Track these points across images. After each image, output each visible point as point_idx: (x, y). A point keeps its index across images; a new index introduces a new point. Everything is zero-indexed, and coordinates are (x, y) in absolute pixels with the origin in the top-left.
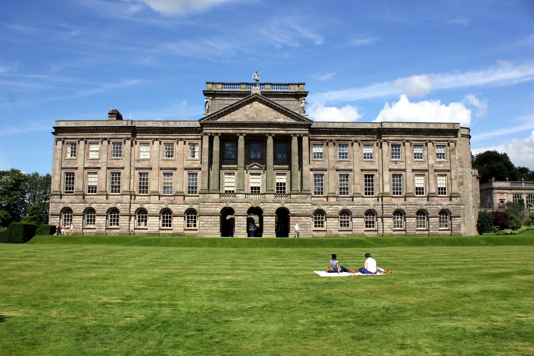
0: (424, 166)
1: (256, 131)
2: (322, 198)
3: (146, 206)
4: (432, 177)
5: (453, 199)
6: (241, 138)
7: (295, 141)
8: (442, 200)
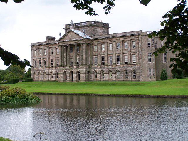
0: (127, 52)
1: (72, 43)
2: (96, 66)
3: (52, 71)
4: (129, 56)
5: (136, 65)
7: (82, 45)
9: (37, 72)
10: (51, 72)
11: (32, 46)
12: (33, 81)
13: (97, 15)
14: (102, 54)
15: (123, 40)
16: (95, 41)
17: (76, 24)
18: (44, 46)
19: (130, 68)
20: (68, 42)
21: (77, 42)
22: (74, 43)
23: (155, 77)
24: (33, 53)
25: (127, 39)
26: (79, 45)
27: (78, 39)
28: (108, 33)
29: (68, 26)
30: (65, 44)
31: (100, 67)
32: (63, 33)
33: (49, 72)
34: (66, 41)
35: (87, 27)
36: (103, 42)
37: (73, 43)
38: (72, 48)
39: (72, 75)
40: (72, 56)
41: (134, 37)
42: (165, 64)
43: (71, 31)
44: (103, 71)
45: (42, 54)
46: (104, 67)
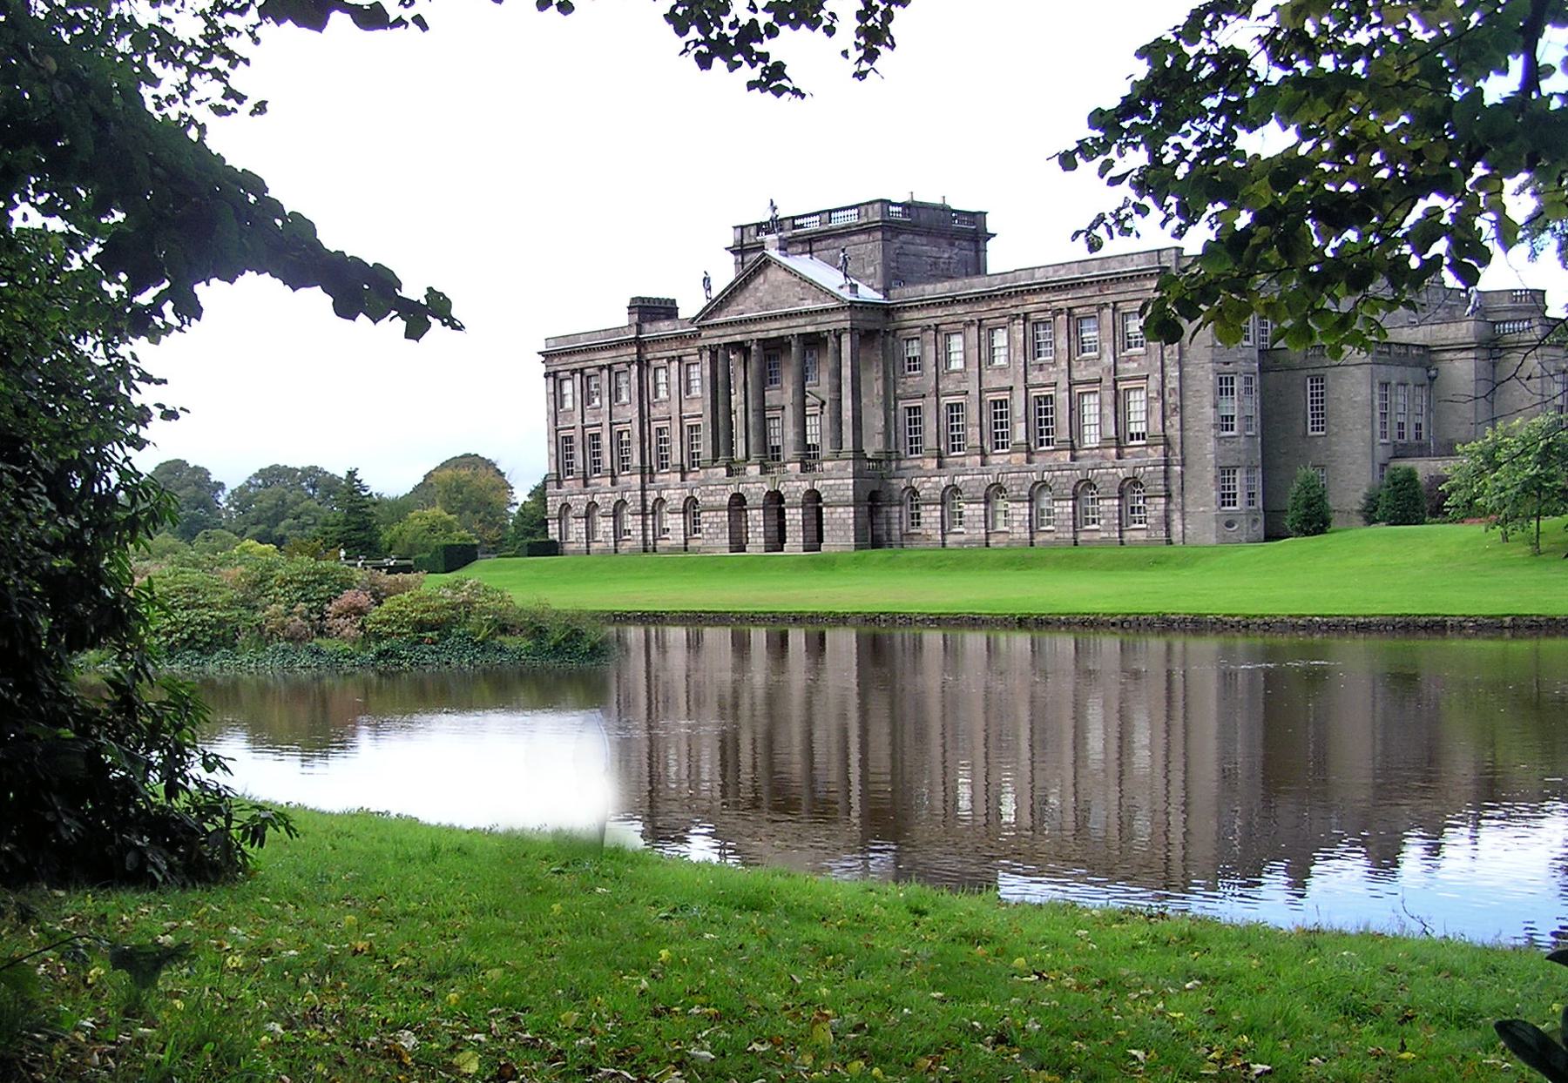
1: (774, 330)
3: (665, 494)
4: (1109, 396)
6: (754, 347)
8: (1134, 456)
9: (579, 504)
10: (660, 501)
11: (547, 356)
12: (556, 554)
13: (797, 92)
14: (951, 388)
15: (1071, 304)
16: (907, 316)
17: (794, 218)
18: (614, 353)
19: (1114, 472)
20: (752, 328)
21: (801, 321)
22: (789, 332)
23: (1261, 518)
24: (557, 398)
25: (1095, 300)
26: (814, 342)
27: (809, 305)
28: (979, 268)
29: (753, 231)
30: (738, 338)
31: (940, 466)
32: (725, 272)
33: (650, 503)
34: (741, 322)
35: (863, 237)
36: (951, 319)
37: (782, 333)
38: (776, 357)
39: (781, 513)
40: (775, 403)
41: (1132, 286)
42: (1320, 441)
43: (767, 263)
44: (955, 490)
45: (606, 400)
46: (963, 465)
